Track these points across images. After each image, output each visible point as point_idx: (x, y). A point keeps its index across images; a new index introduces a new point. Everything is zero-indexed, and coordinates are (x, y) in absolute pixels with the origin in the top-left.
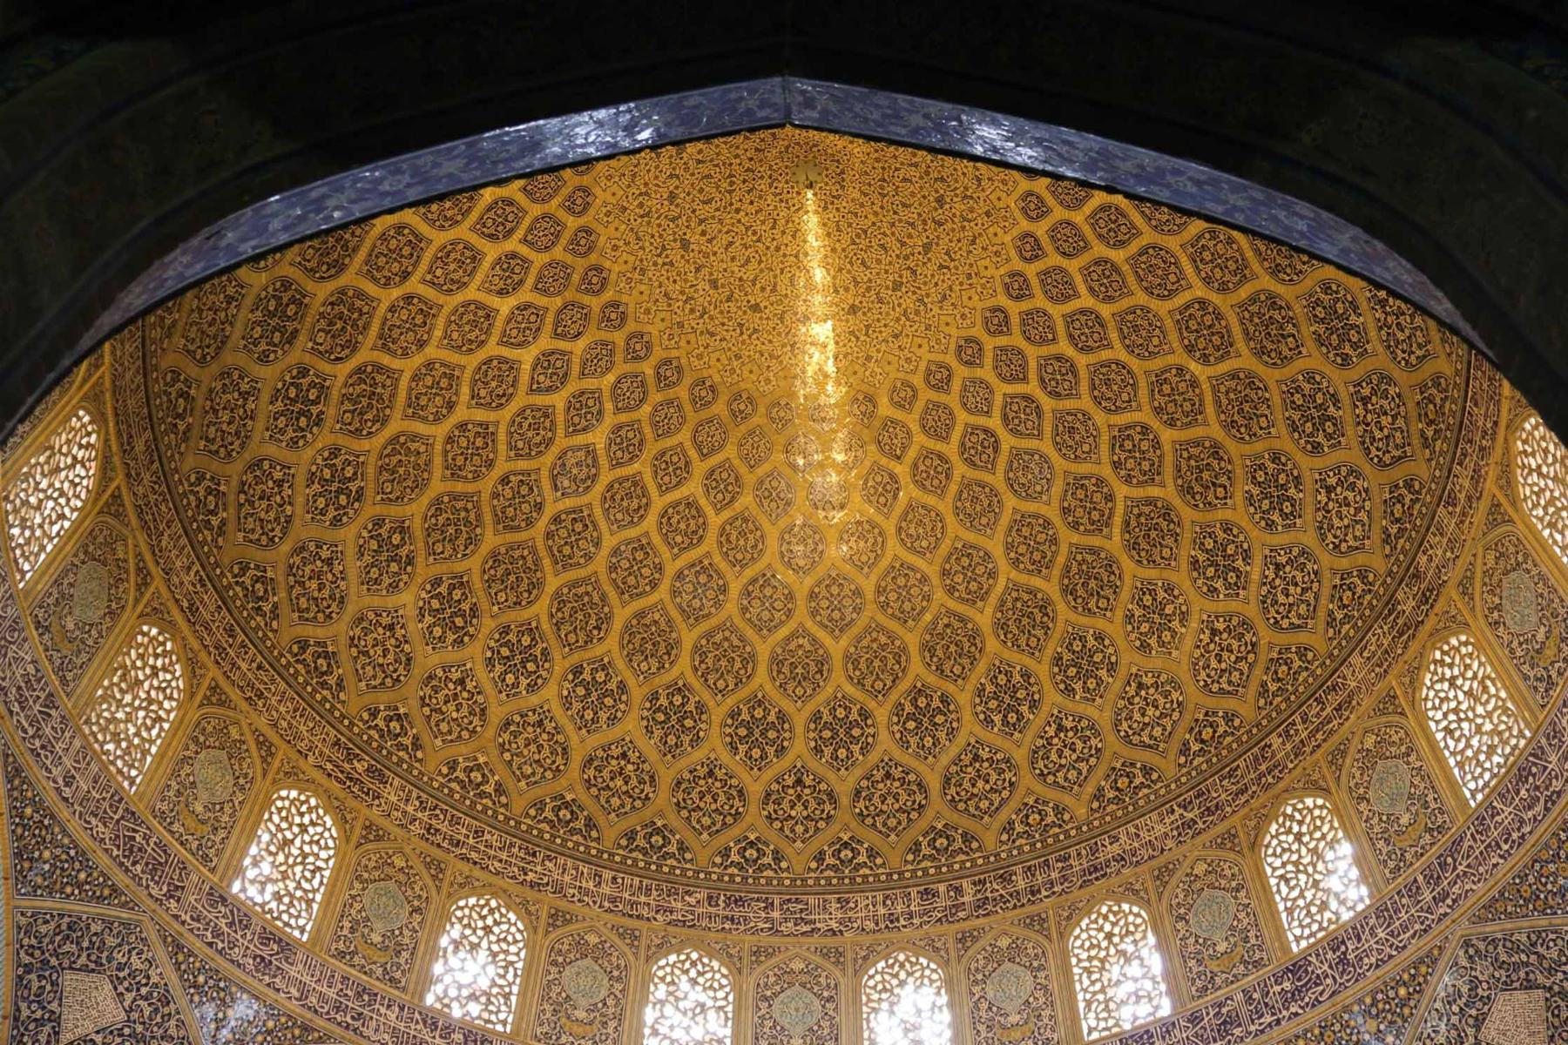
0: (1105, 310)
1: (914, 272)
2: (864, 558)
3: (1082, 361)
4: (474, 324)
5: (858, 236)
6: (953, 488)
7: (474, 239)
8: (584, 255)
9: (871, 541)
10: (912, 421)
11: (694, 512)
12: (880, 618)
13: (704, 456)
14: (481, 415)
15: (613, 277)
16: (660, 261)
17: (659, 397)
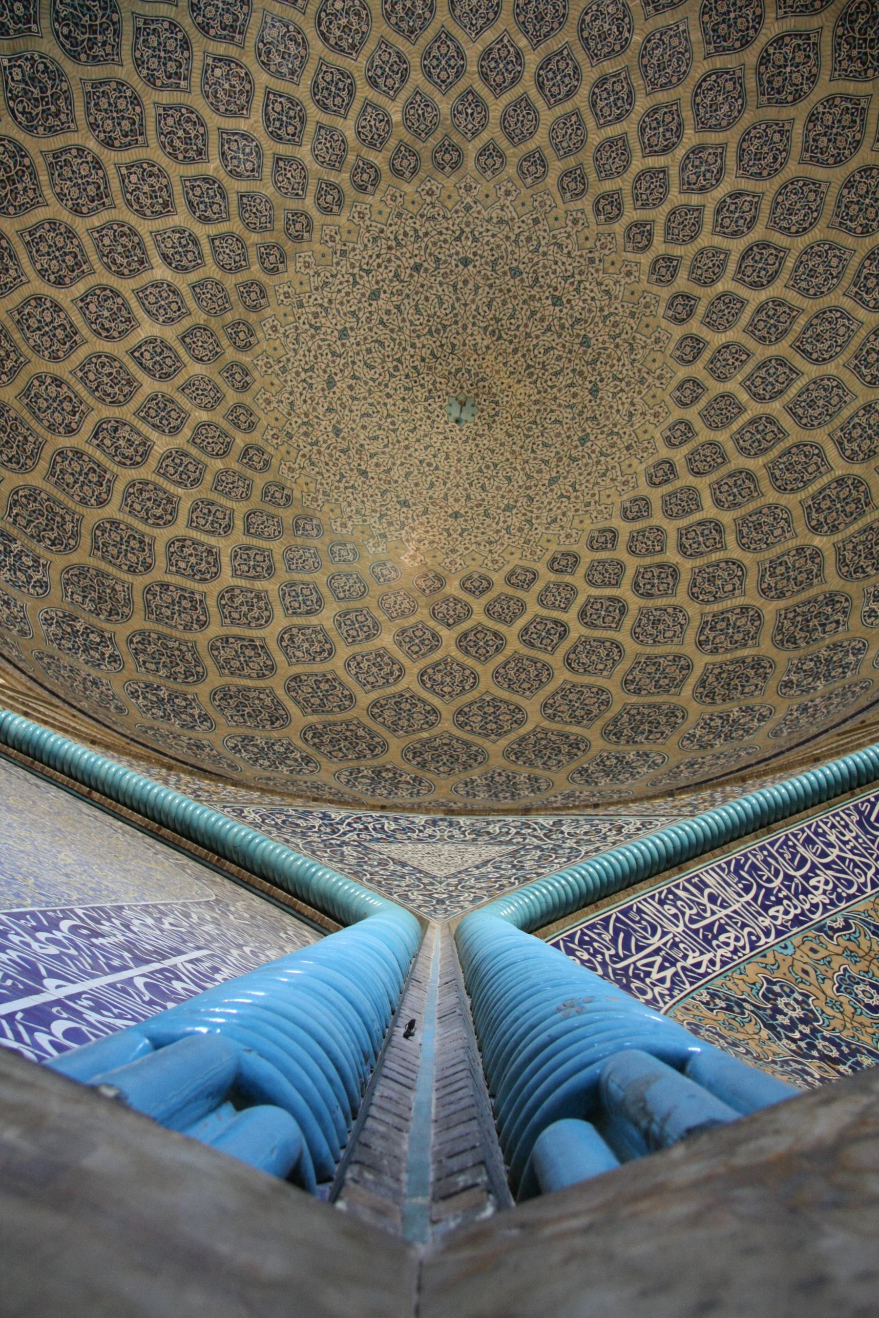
0: (727, 518)
1: (531, 499)
2: (371, 679)
3: (687, 566)
4: (127, 254)
5: (488, 467)
6: (500, 659)
7: (177, 189)
8: (248, 307)
9: (387, 670)
10: (478, 605)
11: (211, 559)
12: (367, 720)
13: (247, 531)
14: (77, 319)
15: (258, 349)
16: (303, 375)
17: (235, 466)
